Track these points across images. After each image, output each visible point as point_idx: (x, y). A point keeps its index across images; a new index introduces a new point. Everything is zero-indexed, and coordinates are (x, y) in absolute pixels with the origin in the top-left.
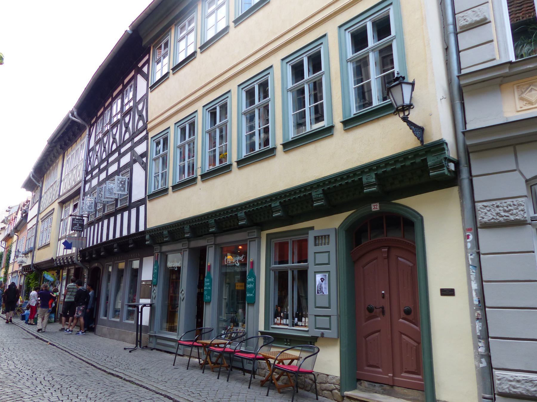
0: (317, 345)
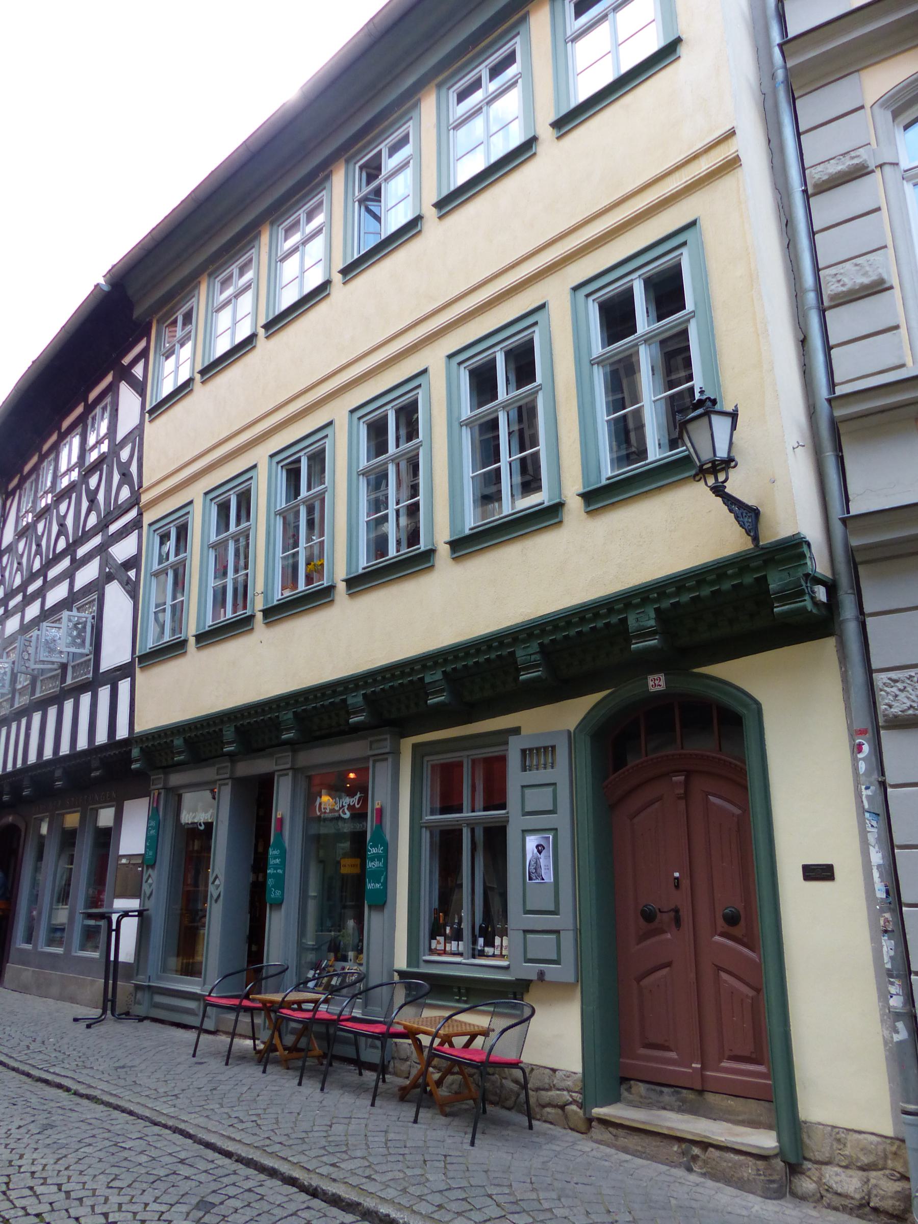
0: (528, 999)
